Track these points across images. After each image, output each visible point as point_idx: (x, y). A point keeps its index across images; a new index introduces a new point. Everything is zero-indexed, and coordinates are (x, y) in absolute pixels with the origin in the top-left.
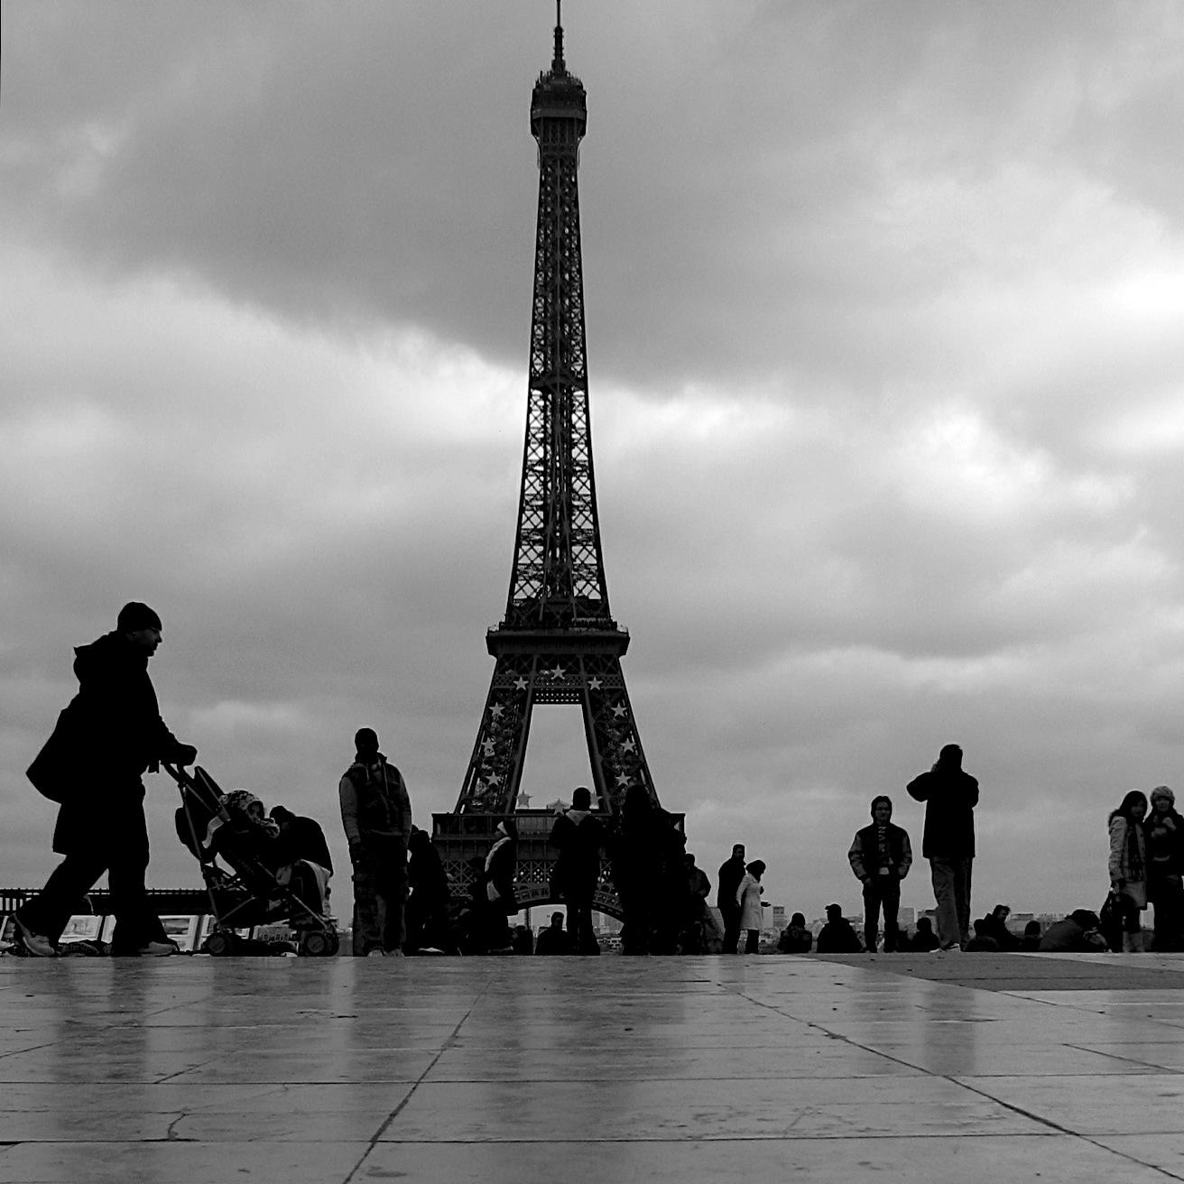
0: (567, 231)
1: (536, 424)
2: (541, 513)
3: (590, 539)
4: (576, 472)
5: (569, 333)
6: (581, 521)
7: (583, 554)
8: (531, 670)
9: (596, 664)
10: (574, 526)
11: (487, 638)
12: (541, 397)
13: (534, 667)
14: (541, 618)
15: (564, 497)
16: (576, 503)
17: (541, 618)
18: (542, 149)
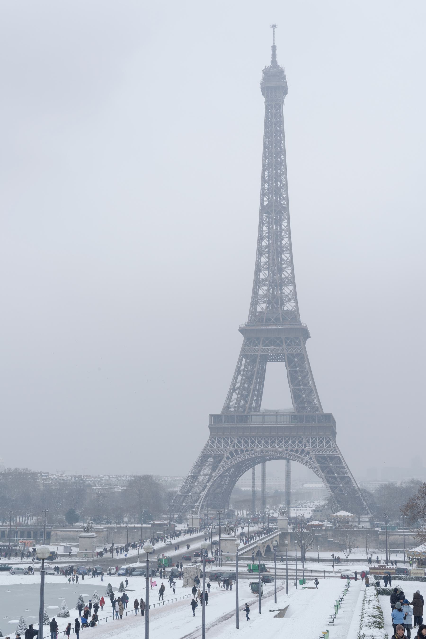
0: (279, 138)
1: (265, 228)
2: (267, 272)
3: (291, 282)
4: (283, 251)
5: (280, 185)
6: (286, 274)
7: (287, 290)
8: (259, 344)
9: (291, 341)
10: (283, 276)
11: (239, 330)
12: (267, 217)
13: (261, 344)
14: (264, 321)
15: (276, 262)
16: (284, 266)
17: (264, 321)
18: (267, 101)
